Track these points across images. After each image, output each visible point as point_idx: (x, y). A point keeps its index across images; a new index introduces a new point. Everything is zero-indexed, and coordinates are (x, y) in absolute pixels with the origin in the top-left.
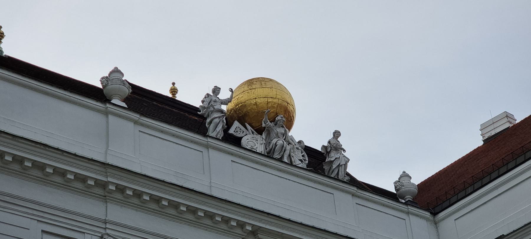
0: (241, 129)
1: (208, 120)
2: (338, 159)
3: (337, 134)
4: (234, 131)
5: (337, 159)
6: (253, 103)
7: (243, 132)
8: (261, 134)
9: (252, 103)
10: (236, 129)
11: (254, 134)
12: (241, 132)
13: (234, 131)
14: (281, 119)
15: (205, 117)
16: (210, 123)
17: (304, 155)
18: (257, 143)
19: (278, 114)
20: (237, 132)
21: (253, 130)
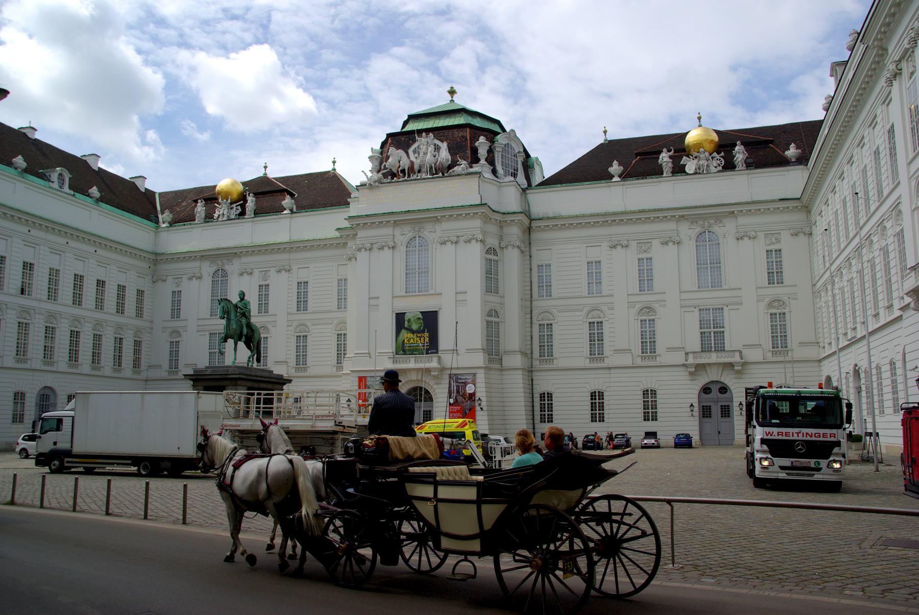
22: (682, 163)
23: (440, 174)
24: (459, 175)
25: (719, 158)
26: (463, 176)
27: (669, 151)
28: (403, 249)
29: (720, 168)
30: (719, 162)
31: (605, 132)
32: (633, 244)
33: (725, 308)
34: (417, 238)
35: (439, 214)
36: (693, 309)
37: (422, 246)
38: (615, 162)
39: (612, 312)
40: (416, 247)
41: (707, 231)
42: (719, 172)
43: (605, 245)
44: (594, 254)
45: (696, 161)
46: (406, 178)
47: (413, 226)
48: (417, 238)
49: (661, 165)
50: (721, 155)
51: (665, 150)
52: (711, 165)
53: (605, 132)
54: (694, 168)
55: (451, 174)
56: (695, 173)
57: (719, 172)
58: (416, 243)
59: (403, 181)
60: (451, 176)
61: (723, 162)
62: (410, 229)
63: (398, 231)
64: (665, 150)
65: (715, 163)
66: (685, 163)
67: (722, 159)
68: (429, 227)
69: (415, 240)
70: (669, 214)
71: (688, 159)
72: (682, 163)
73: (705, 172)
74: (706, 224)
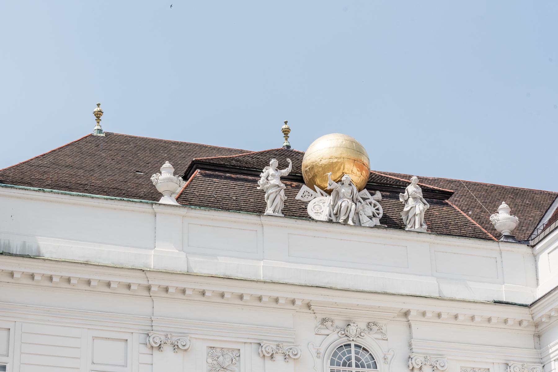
0: (309, 193)
1: (266, 196)
2: (414, 208)
3: (414, 181)
4: (302, 197)
5: (413, 208)
6: (319, 165)
7: (312, 195)
8: (330, 194)
9: (318, 165)
10: (303, 194)
11: (324, 195)
12: (309, 196)
13: (302, 197)
14: (345, 179)
15: (265, 191)
16: (268, 198)
17: (378, 208)
18: (324, 206)
19: (344, 173)
20: (305, 196)
21: (322, 192)
22: (298, 197)
25: (374, 202)
27: (282, 166)
29: (376, 221)
30: (374, 210)
31: (98, 115)
38: (167, 164)
41: (353, 346)
42: (376, 226)
45: (329, 199)
49: (263, 192)
50: (375, 196)
51: (274, 162)
52: (361, 212)
53: (98, 115)
54: (327, 212)
56: (330, 221)
57: (376, 226)
61: (381, 211)
64: (274, 162)
65: (370, 210)
66: (305, 200)
67: (379, 206)
70: (284, 293)
71: (311, 191)
72: (298, 197)
73: (350, 222)
74: (352, 330)
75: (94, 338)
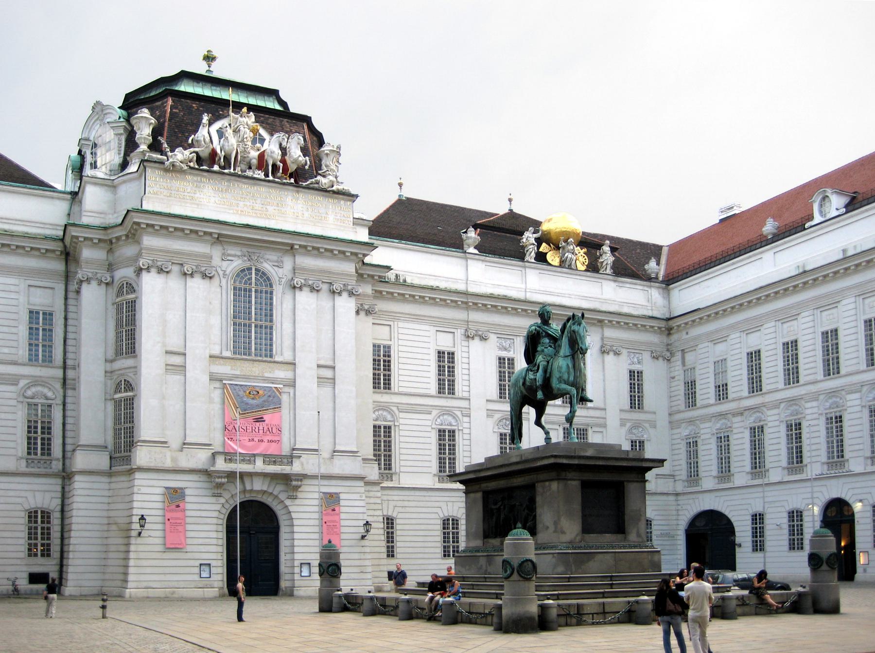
23: (292, 180)
24: (325, 191)
26: (331, 194)
28: (227, 285)
32: (493, 338)
33: (590, 429)
34: (253, 272)
35: (297, 242)
36: (557, 427)
37: (261, 285)
39: (466, 419)
40: (250, 284)
43: (459, 333)
44: (445, 342)
46: (232, 170)
47: (245, 250)
48: (253, 272)
55: (311, 185)
58: (250, 279)
59: (230, 174)
60: (313, 189)
62: (239, 253)
63: (216, 253)
68: (273, 256)
69: (251, 274)
75: (437, 331)
